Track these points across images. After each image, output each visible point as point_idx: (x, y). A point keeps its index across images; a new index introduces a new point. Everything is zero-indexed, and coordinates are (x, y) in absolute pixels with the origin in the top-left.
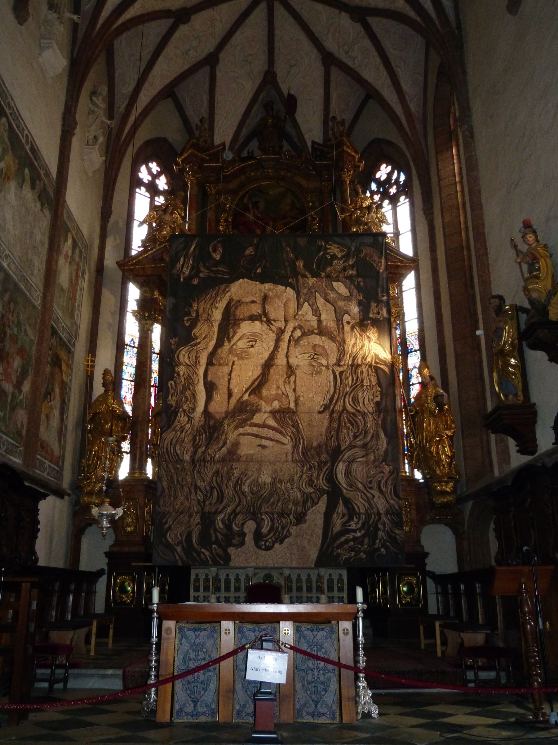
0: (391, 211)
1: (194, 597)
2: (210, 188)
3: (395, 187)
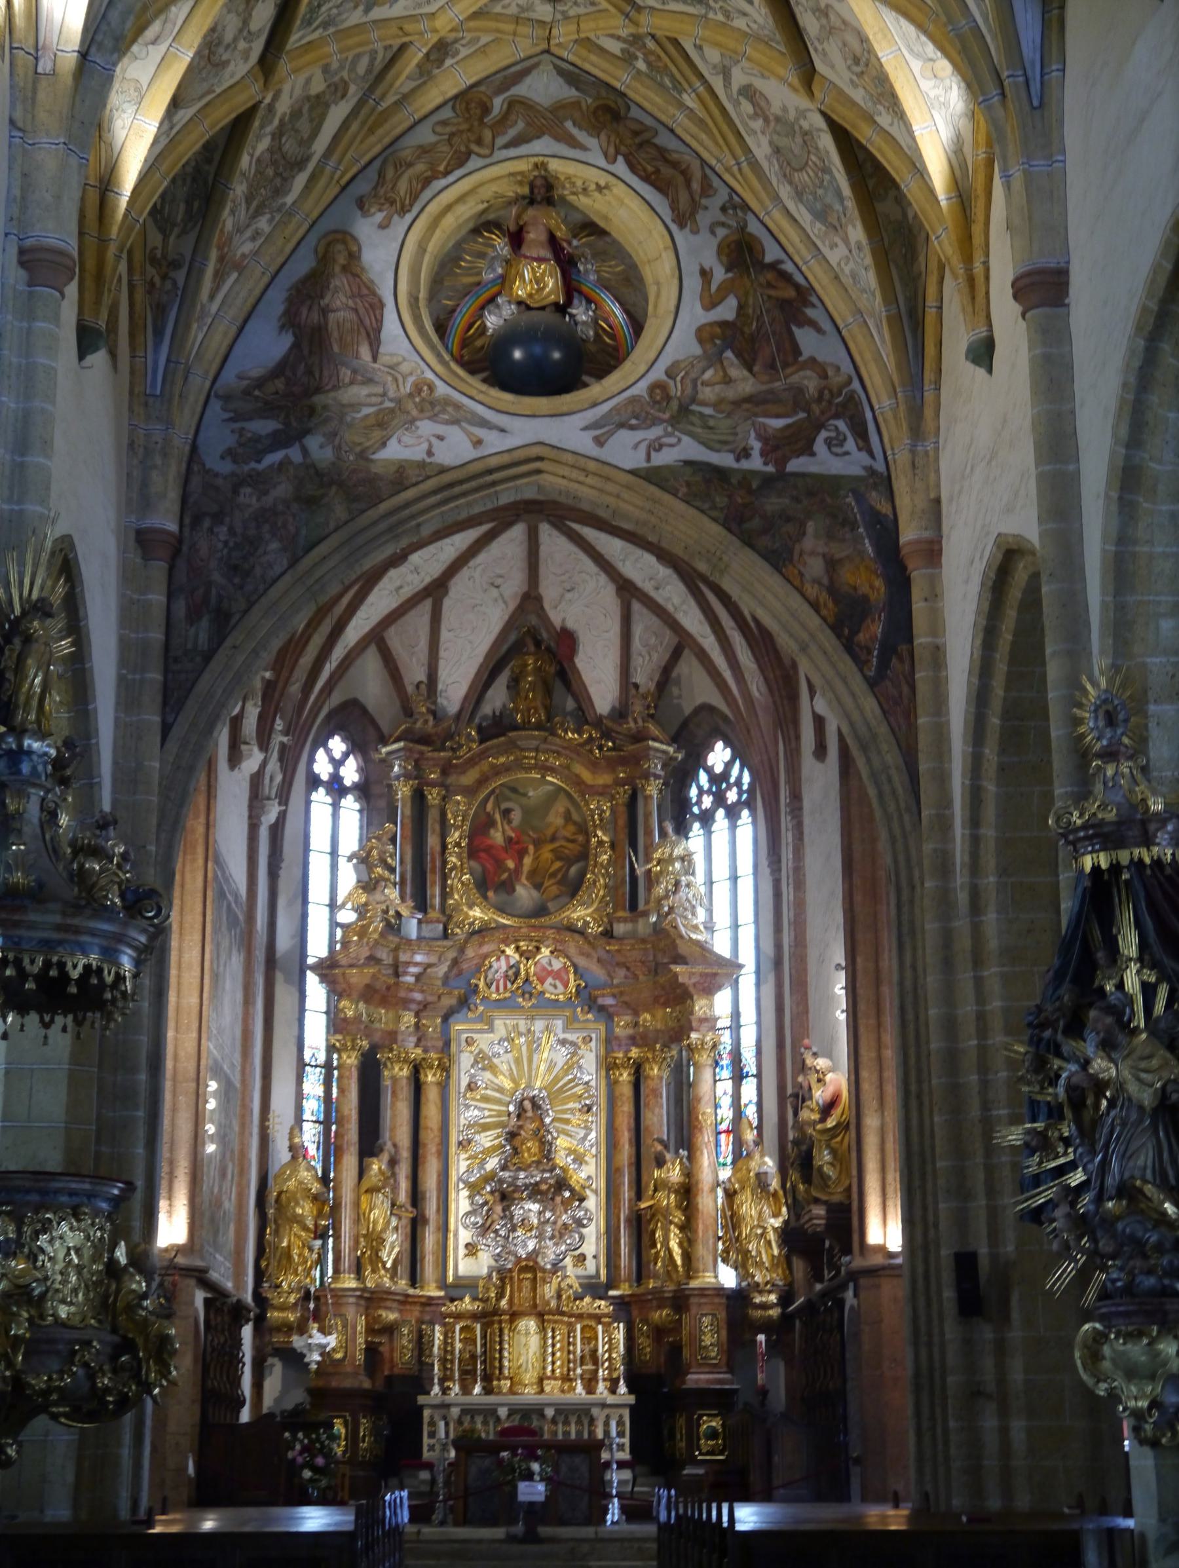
3: (735, 789)
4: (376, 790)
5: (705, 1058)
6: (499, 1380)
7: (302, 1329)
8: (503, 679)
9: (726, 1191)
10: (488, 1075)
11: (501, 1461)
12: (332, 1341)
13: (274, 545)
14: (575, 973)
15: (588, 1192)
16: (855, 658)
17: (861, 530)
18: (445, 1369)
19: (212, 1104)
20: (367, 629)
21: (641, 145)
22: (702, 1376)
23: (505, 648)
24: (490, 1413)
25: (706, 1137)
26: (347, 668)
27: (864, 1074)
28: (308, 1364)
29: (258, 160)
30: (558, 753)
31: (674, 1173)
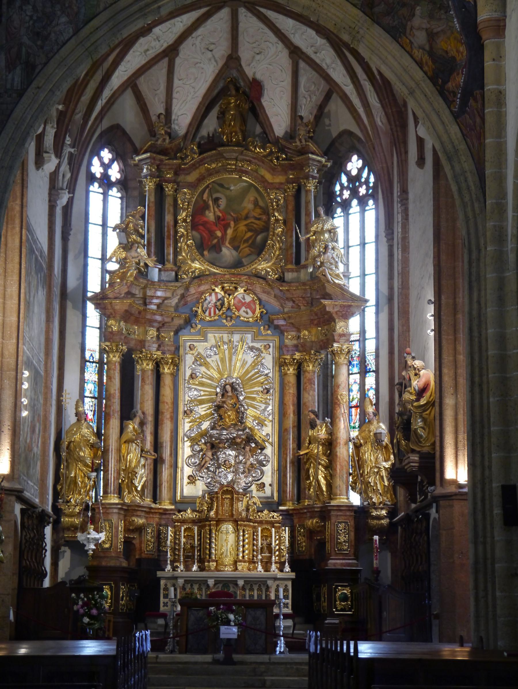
0: (359, 213)
1: (164, 603)
2: (168, 188)
3: (364, 187)
4: (132, 184)
5: (342, 360)
6: (209, 562)
7: (83, 529)
8: (214, 113)
9: (355, 444)
10: (203, 369)
11: (209, 613)
12: (102, 536)
13: (63, 19)
14: (260, 304)
15: (267, 444)
16: (445, 99)
17: (452, 12)
18: (175, 554)
19: (26, 386)
20: (125, 78)
22: (338, 561)
23: (216, 92)
24: (203, 582)
25: (343, 410)
26: (113, 104)
27: (445, 371)
28: (87, 551)
30: (250, 161)
31: (322, 433)
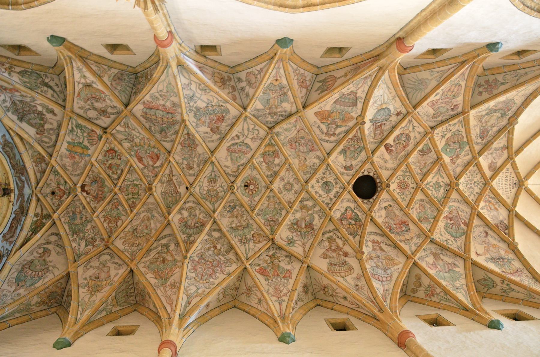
21: (18, 221)
29: (35, 106)
